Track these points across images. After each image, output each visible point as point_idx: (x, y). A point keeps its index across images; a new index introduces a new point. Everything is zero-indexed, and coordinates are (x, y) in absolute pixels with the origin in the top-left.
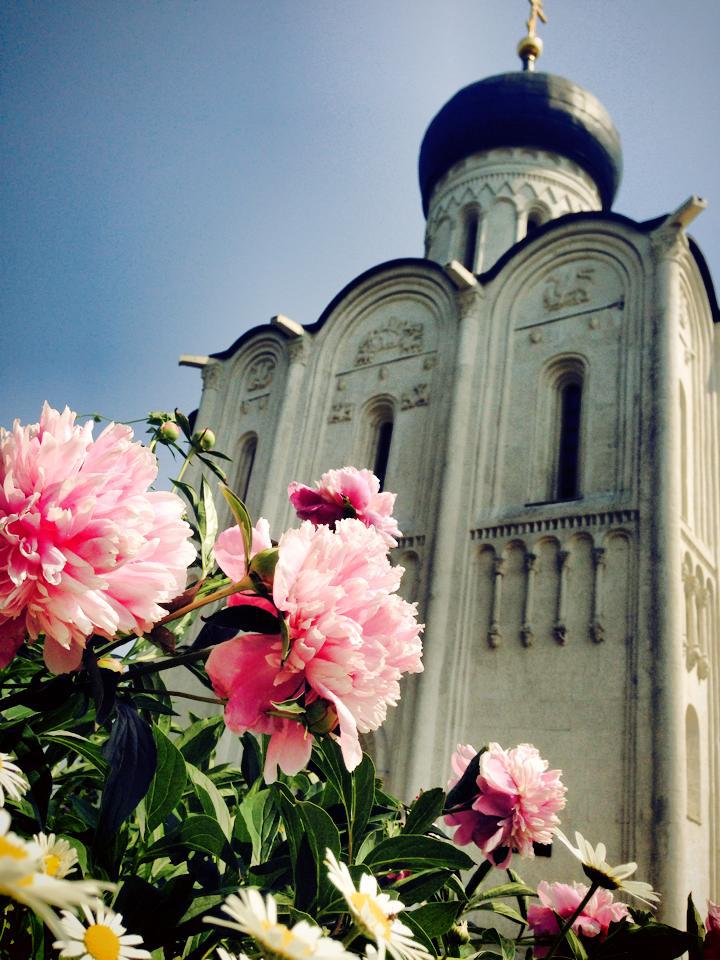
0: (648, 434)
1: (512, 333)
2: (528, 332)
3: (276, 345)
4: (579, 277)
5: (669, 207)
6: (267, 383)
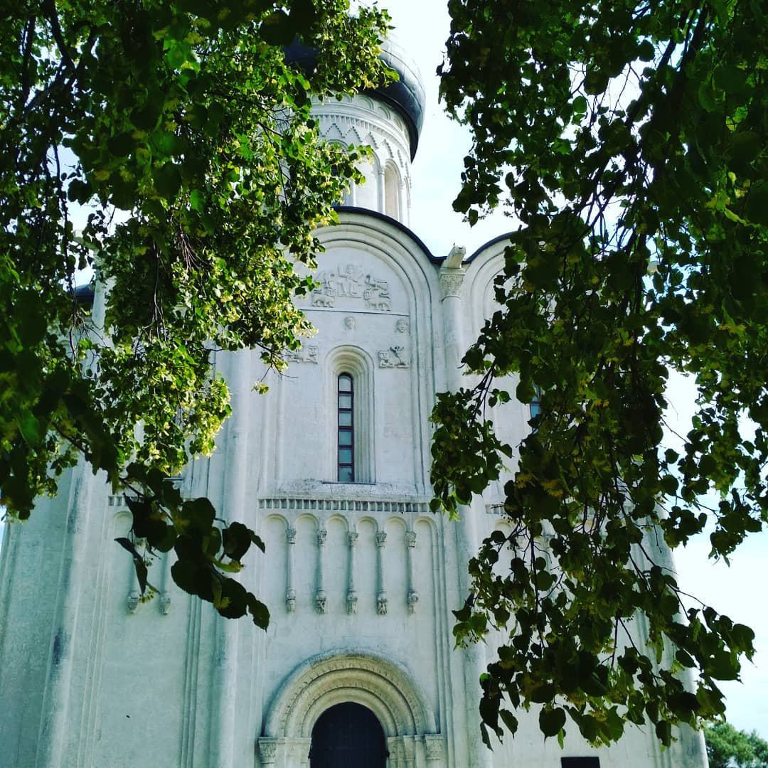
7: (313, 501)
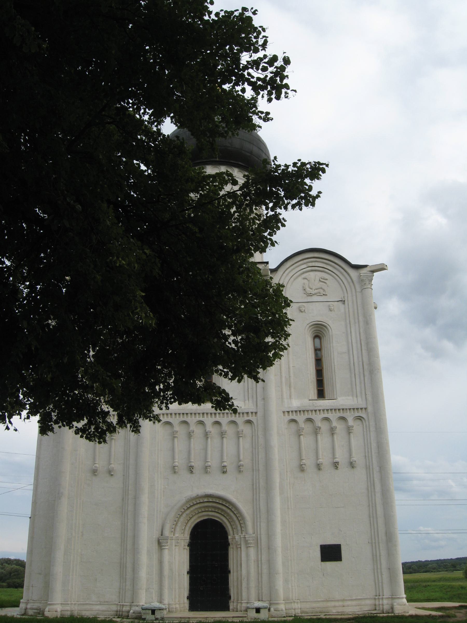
4: (320, 280)
5: (371, 261)
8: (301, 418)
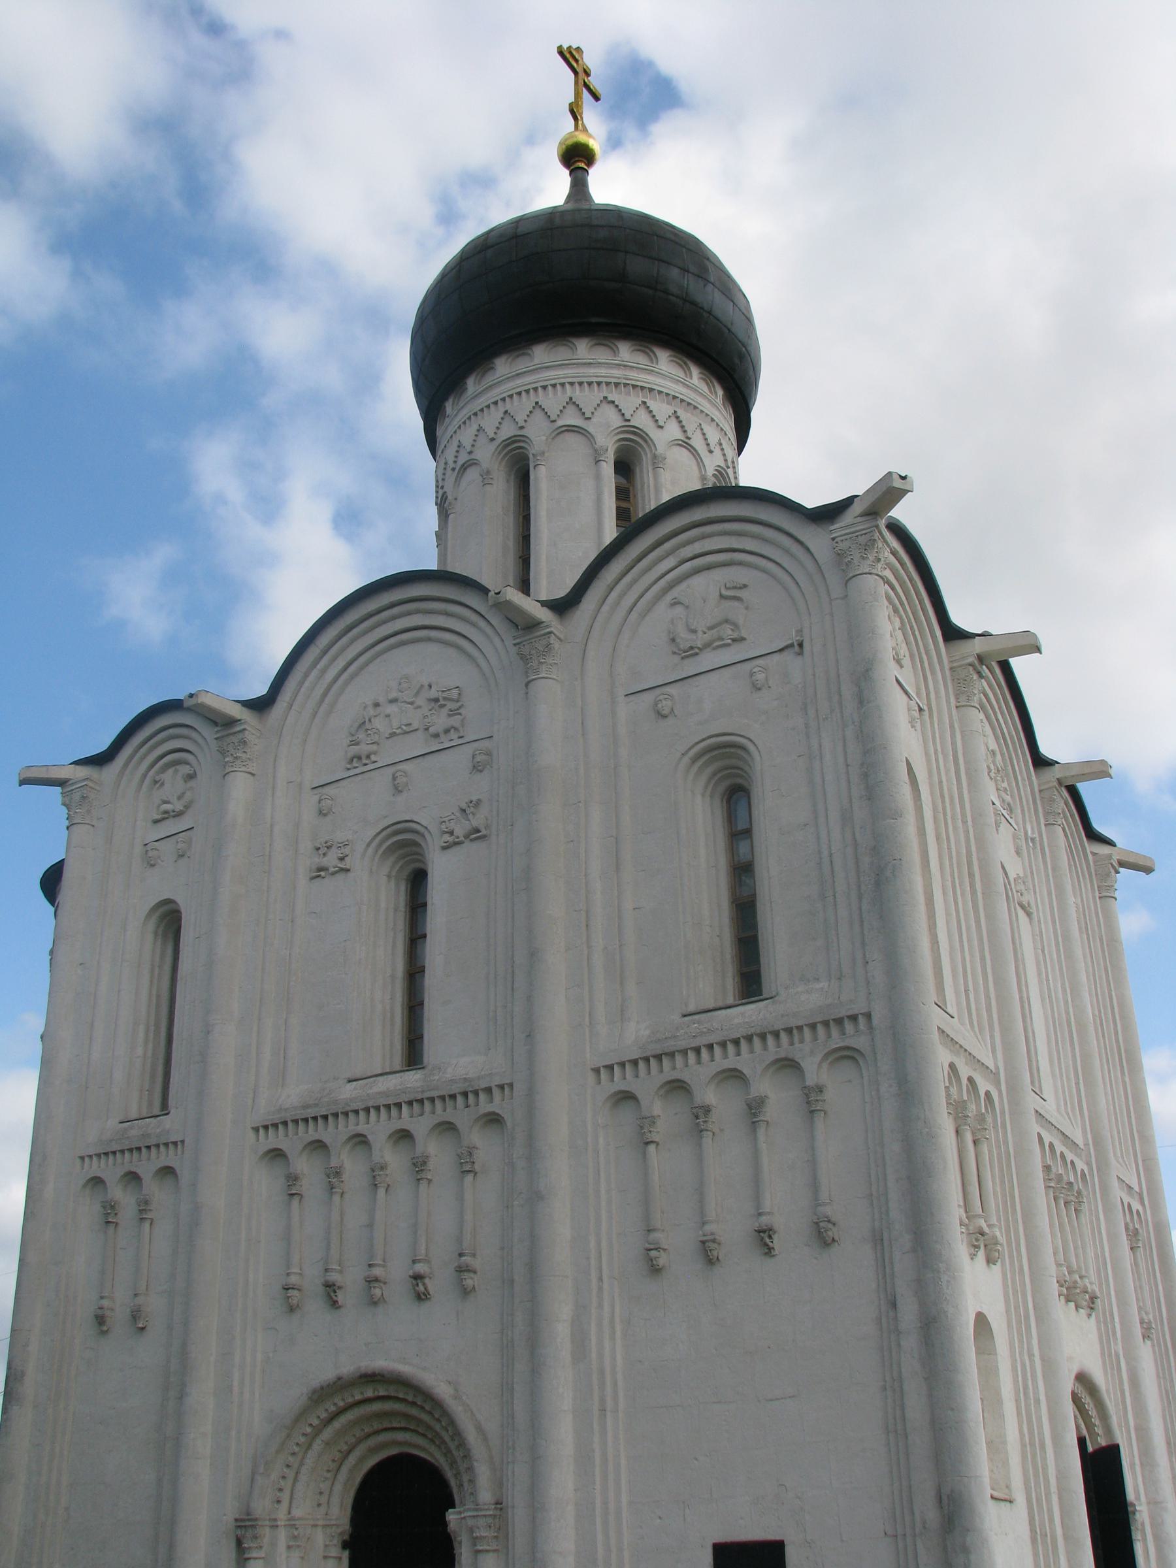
0: (875, 880)
1: (621, 698)
2: (649, 697)
3: (194, 735)
4: (721, 596)
6: (187, 807)
7: (325, 1117)
8: (646, 1084)
